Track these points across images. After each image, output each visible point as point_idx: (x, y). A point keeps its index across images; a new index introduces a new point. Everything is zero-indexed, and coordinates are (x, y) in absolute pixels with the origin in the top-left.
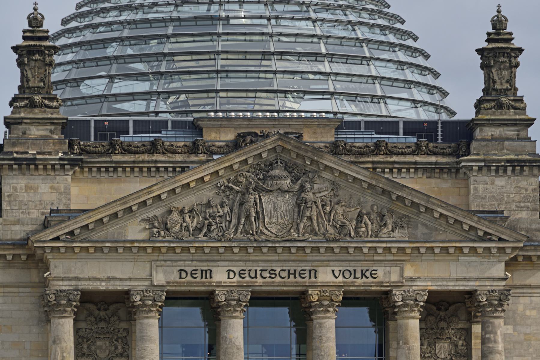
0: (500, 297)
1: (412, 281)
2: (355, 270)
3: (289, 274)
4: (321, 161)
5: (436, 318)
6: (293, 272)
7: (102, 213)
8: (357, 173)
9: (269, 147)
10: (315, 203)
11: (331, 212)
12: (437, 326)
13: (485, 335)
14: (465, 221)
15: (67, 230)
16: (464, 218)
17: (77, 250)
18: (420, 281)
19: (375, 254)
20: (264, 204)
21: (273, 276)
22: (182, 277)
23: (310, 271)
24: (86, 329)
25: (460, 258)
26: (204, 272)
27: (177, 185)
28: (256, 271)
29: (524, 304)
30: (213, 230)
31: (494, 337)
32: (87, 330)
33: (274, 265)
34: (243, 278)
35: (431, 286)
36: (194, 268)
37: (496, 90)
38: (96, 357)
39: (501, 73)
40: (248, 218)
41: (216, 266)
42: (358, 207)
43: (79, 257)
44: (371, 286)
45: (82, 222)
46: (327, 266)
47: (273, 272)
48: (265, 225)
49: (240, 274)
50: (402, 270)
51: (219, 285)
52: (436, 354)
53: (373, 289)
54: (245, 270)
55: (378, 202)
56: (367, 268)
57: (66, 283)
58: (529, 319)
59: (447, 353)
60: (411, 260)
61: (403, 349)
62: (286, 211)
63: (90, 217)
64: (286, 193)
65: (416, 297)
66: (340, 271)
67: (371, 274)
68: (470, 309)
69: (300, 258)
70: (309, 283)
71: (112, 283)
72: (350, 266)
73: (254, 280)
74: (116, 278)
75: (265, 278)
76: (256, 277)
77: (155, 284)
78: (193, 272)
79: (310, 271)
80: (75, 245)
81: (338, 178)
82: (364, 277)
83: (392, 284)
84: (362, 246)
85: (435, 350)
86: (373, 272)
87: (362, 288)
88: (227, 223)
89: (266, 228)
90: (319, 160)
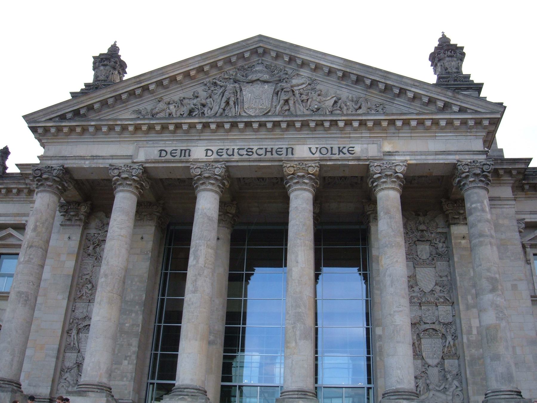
0: (482, 169)
1: (390, 155)
2: (332, 148)
3: (266, 152)
4: (298, 56)
5: (416, 223)
6: (270, 150)
7: (93, 100)
8: (332, 63)
9: (251, 48)
10: (293, 91)
11: (308, 100)
12: (417, 229)
13: (471, 205)
14: (439, 97)
15: (59, 114)
16: (438, 95)
17: (66, 130)
18: (399, 155)
19: (351, 131)
20: (244, 93)
21: (251, 153)
22: (162, 156)
23: (287, 149)
24: (95, 234)
25: (437, 135)
26: (183, 151)
27: (164, 77)
28: (233, 149)
29: (496, 214)
30: (195, 116)
31: (481, 206)
32: (96, 235)
33: (251, 144)
34: (221, 156)
35: (410, 160)
36: (175, 148)
37: (449, 73)
38: (99, 257)
39: (451, 63)
40: (227, 103)
41: (195, 146)
42: (334, 96)
43: (69, 141)
44: (348, 160)
45: (74, 107)
46: (304, 144)
47: (250, 150)
48: (244, 111)
49: (217, 152)
50: (380, 147)
51: (196, 161)
52: (417, 256)
53: (350, 163)
54: (223, 149)
55: (353, 93)
56: (344, 146)
57: (54, 162)
58: (503, 226)
59: (429, 255)
60: (388, 138)
61: (385, 218)
62: (265, 99)
63: (82, 102)
64: (265, 84)
65: (395, 170)
66: (317, 148)
67: (348, 151)
68: (447, 212)
69: (277, 137)
70: (285, 158)
71: (95, 161)
72: (327, 144)
73: (232, 157)
74: (99, 156)
75: (242, 155)
76: (233, 155)
77: (135, 161)
78: (173, 152)
79: (287, 149)
80: (63, 124)
81: (314, 74)
82: (341, 153)
83: (370, 158)
84: (338, 119)
85: (417, 252)
86: (350, 149)
87: (340, 163)
88: (209, 110)
89: (245, 112)
90: (296, 55)
